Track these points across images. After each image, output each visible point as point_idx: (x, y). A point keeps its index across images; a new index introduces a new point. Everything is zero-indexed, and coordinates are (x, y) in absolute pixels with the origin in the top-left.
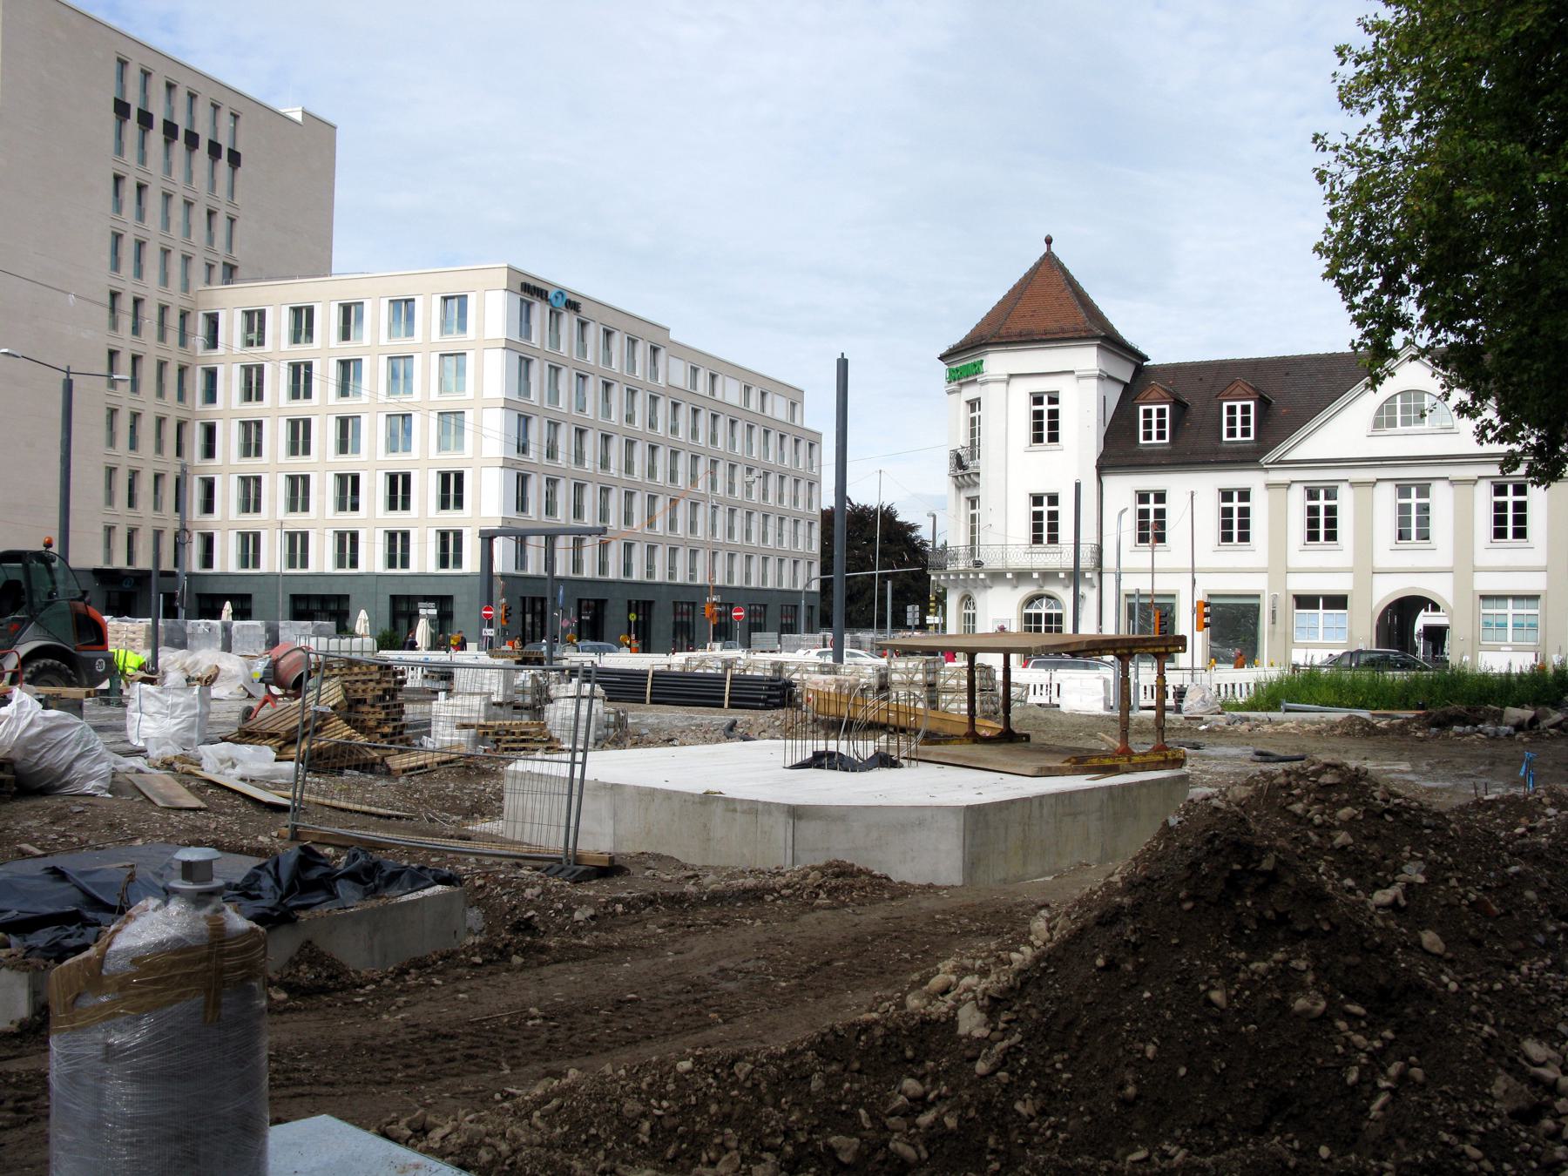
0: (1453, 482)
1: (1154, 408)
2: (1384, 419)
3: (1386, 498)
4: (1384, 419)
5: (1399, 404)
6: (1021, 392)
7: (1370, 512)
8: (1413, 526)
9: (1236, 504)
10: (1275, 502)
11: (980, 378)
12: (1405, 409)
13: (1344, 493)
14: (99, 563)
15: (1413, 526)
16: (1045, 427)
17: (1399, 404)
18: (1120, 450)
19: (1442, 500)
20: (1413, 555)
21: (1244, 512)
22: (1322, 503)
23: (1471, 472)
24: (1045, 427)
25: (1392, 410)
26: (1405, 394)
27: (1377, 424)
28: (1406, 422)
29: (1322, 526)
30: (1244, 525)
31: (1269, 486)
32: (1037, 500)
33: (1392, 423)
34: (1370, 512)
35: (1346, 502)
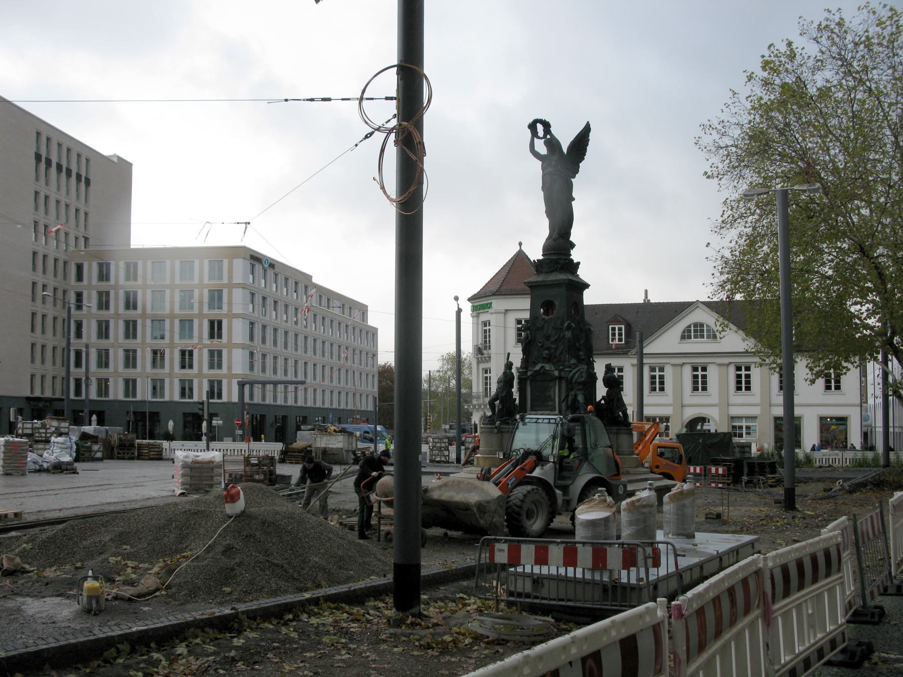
0: (719, 365)
2: (685, 335)
3: (687, 372)
4: (685, 335)
5: (692, 328)
7: (678, 379)
8: (699, 384)
12: (695, 331)
14: (28, 394)
15: (699, 384)
17: (692, 328)
19: (713, 374)
20: (700, 398)
22: (657, 373)
23: (726, 360)
25: (689, 331)
26: (696, 325)
28: (696, 337)
33: (689, 337)
34: (678, 379)
35: (669, 374)
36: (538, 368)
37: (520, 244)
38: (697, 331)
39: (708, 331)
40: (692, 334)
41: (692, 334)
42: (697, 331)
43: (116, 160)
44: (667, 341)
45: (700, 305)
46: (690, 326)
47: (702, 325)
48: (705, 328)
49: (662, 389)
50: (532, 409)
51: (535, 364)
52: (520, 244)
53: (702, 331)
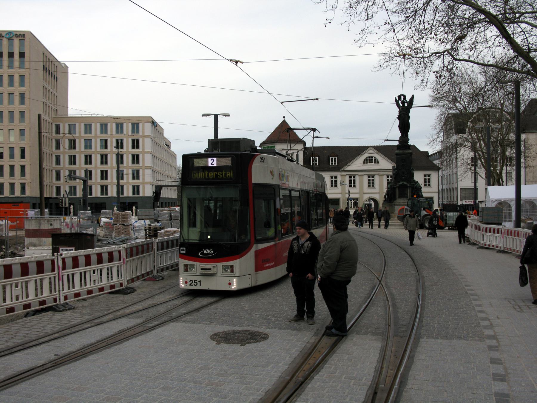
0: (379, 175)
2: (365, 162)
3: (366, 179)
7: (362, 181)
9: (334, 179)
12: (369, 160)
15: (371, 184)
25: (367, 160)
26: (369, 157)
27: (364, 163)
28: (369, 162)
29: (352, 184)
31: (342, 175)
33: (367, 162)
34: (362, 181)
36: (401, 183)
37: (284, 117)
38: (371, 160)
39: (375, 160)
43: (63, 65)
44: (357, 164)
45: (372, 148)
47: (372, 157)
49: (373, 186)
50: (399, 197)
51: (399, 182)
52: (284, 117)
53: (372, 160)
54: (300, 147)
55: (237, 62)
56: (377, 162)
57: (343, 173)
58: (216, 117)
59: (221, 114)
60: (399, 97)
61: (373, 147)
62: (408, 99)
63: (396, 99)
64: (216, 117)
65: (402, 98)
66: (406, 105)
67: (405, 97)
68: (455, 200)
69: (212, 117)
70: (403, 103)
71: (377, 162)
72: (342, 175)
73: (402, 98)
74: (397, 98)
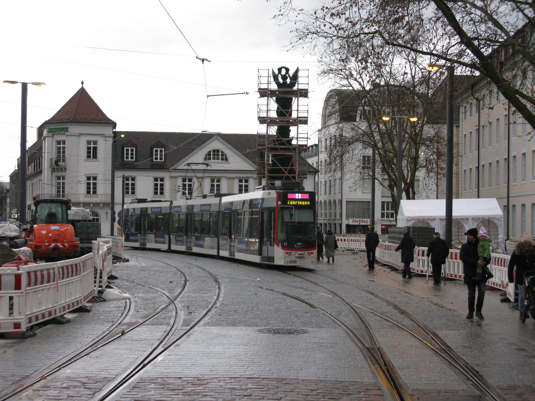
0: (229, 178)
1: (130, 149)
2: (208, 156)
5: (212, 153)
6: (83, 141)
9: (159, 182)
10: (171, 183)
11: (67, 133)
12: (214, 155)
13: (195, 180)
16: (92, 153)
17: (212, 153)
18: (119, 163)
21: (162, 185)
24: (92, 153)
25: (210, 155)
26: (214, 151)
30: (162, 189)
31: (171, 177)
32: (89, 178)
37: (82, 83)
38: (216, 154)
39: (222, 155)
40: (212, 157)
41: (220, 157)
42: (216, 154)
46: (210, 152)
47: (218, 151)
48: (220, 153)
52: (82, 83)
53: (218, 155)
54: (108, 131)
55: (203, 60)
56: (225, 158)
57: (174, 174)
58: (25, 86)
59: (34, 84)
60: (280, 70)
61: (220, 135)
62: (291, 73)
63: (273, 72)
64: (25, 86)
65: (283, 72)
66: (288, 81)
67: (287, 70)
68: (338, 217)
69: (19, 87)
70: (284, 78)
71: (225, 158)
72: (171, 177)
73: (283, 72)
74: (277, 72)
